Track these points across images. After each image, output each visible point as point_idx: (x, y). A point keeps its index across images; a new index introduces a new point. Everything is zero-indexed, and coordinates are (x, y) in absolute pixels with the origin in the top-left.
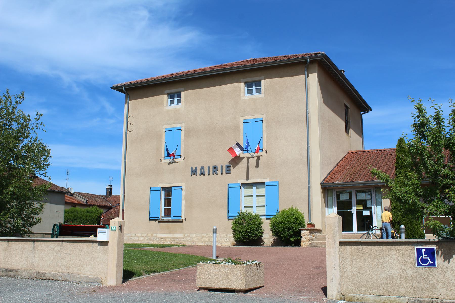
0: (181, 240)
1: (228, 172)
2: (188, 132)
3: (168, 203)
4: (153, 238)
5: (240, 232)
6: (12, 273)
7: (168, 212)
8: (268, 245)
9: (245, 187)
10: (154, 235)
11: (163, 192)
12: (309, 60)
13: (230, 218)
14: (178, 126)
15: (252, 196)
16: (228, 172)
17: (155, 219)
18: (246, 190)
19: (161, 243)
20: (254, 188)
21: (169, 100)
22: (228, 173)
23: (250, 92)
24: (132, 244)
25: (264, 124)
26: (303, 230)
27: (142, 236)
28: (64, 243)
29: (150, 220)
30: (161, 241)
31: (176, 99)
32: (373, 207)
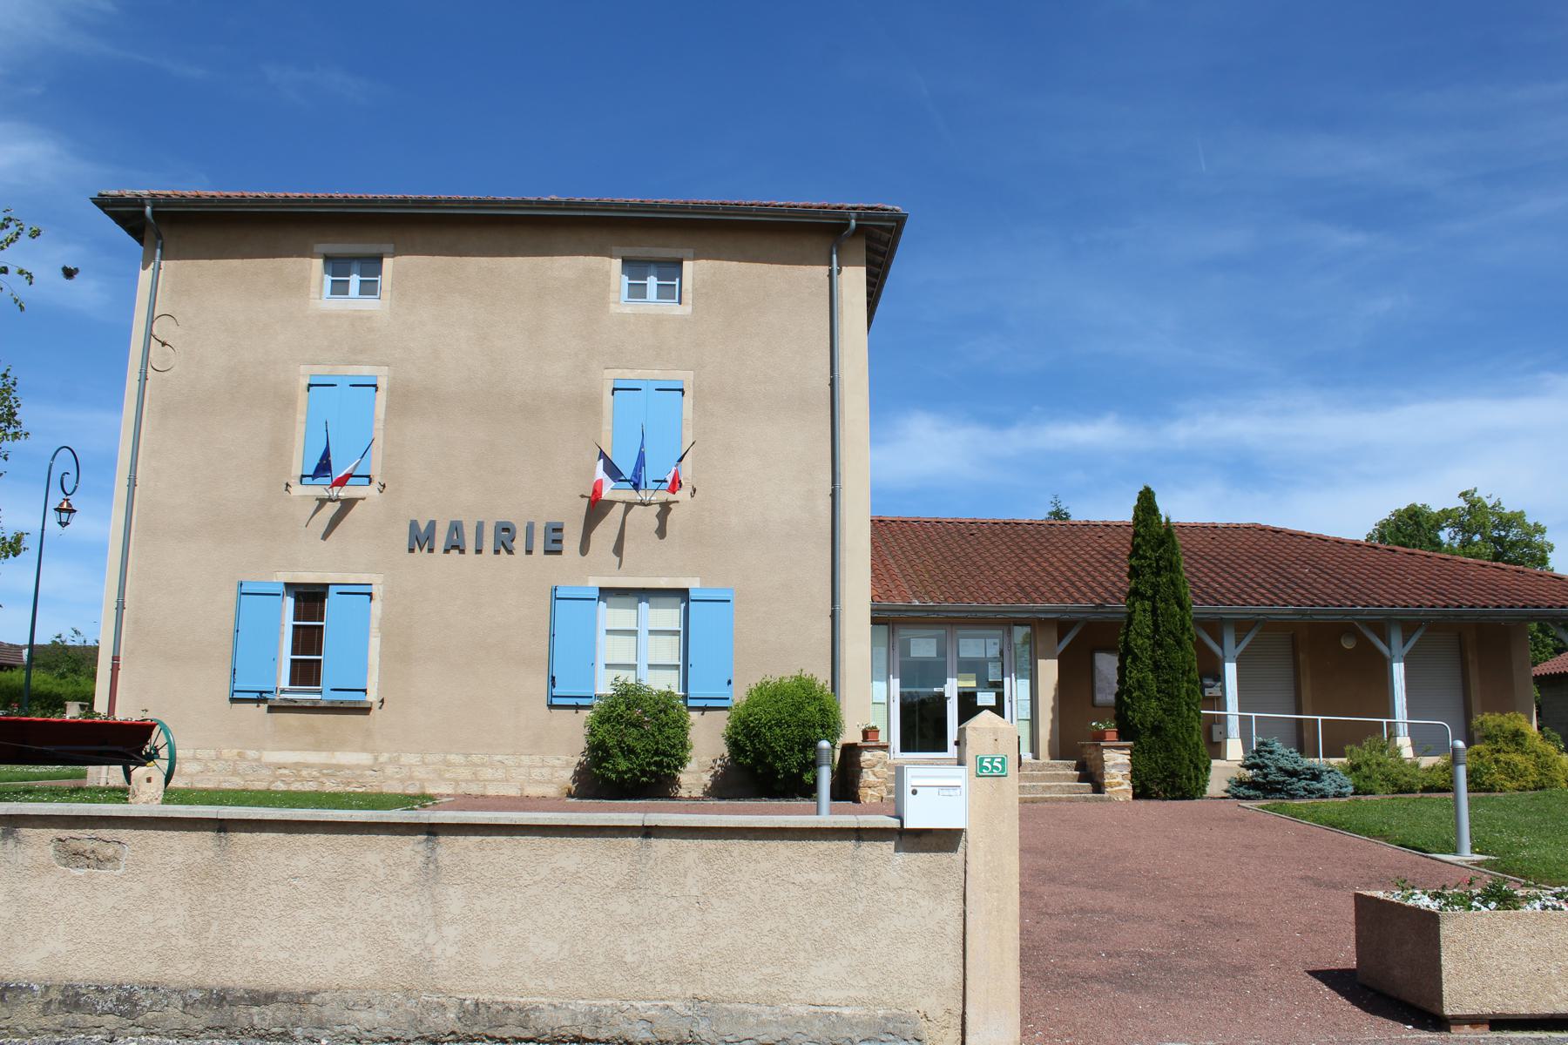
0: (361, 776)
1: (555, 547)
2: (404, 401)
3: (308, 639)
4: (242, 765)
5: (631, 751)
6: (269, 1011)
7: (306, 673)
8: (694, 794)
10: (252, 754)
11: (290, 602)
12: (853, 223)
13: (556, 701)
14: (365, 371)
15: (634, 633)
16: (555, 547)
17: (255, 696)
19: (281, 787)
20: (644, 606)
21: (328, 279)
22: (554, 547)
23: (637, 292)
24: (216, 791)
26: (867, 748)
27: (195, 759)
28: (661, 845)
29: (233, 700)
30: (277, 778)
31: (355, 280)
32: (1007, 680)
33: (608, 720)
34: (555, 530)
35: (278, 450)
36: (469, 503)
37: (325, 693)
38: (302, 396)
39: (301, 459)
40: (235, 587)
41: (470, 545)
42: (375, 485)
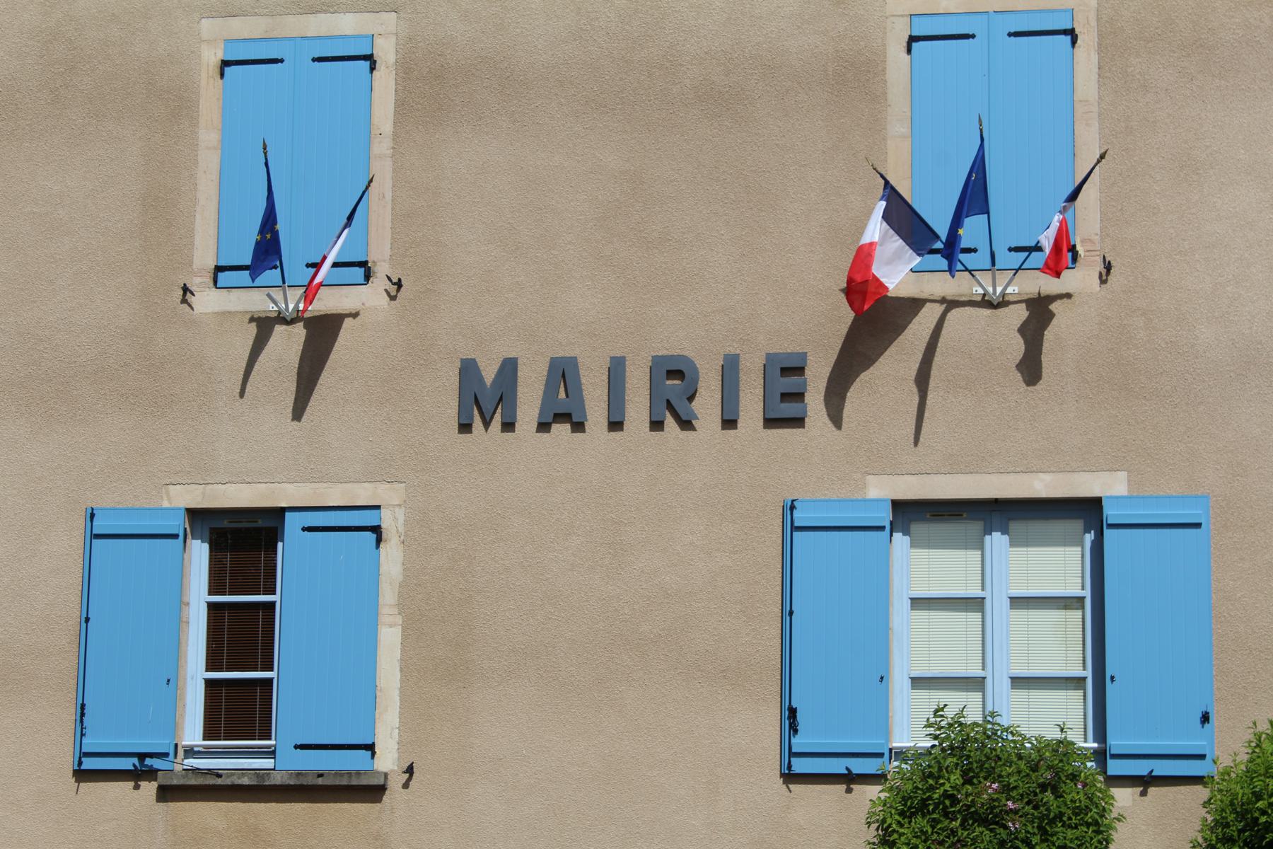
1: (789, 409)
2: (435, 89)
3: (242, 635)
7: (239, 709)
9: (1015, 526)
11: (199, 553)
13: (800, 766)
14: (346, 25)
15: (975, 604)
16: (789, 409)
17: (127, 764)
18: (922, 554)
20: (997, 541)
25: (1086, 56)
29: (82, 775)
33: (922, 808)
34: (786, 371)
35: (162, 210)
36: (587, 316)
37: (282, 758)
38: (210, 92)
39: (212, 228)
40: (80, 522)
41: (596, 415)
42: (379, 284)
